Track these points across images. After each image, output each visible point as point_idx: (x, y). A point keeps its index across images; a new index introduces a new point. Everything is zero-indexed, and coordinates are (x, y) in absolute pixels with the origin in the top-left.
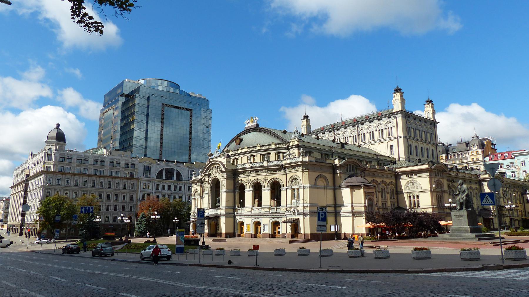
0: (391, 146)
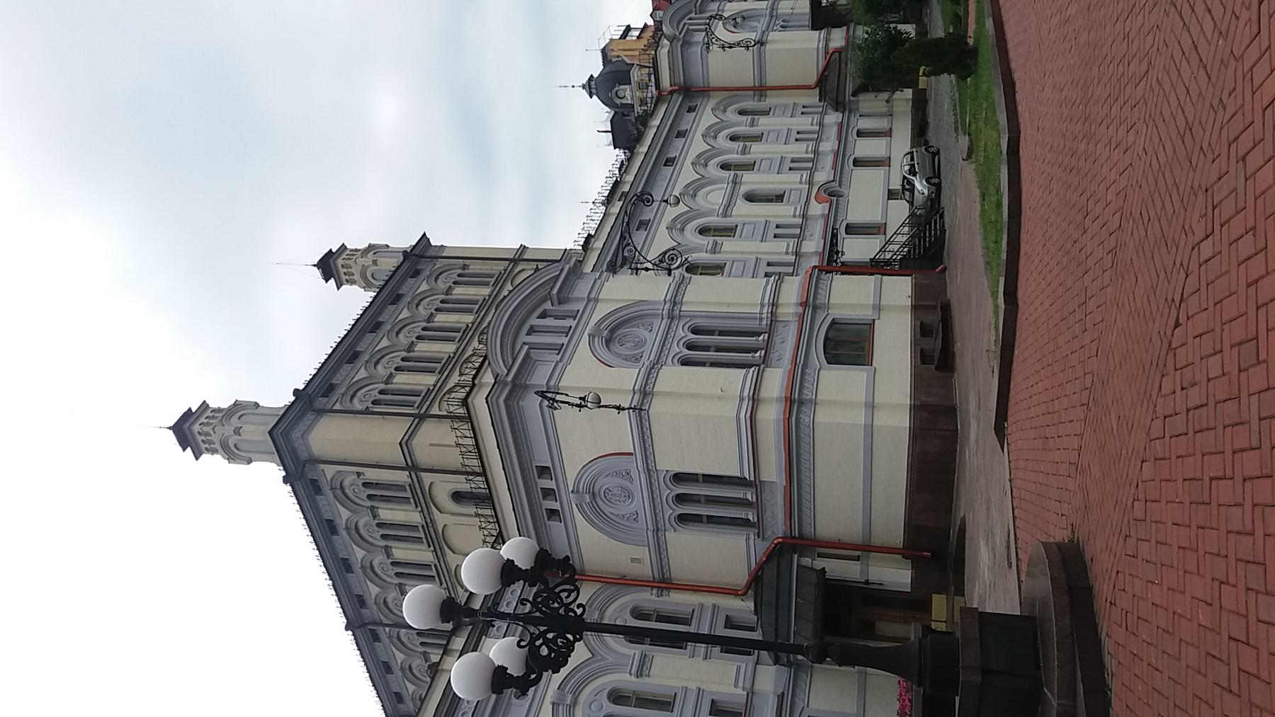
0: (457, 496)
